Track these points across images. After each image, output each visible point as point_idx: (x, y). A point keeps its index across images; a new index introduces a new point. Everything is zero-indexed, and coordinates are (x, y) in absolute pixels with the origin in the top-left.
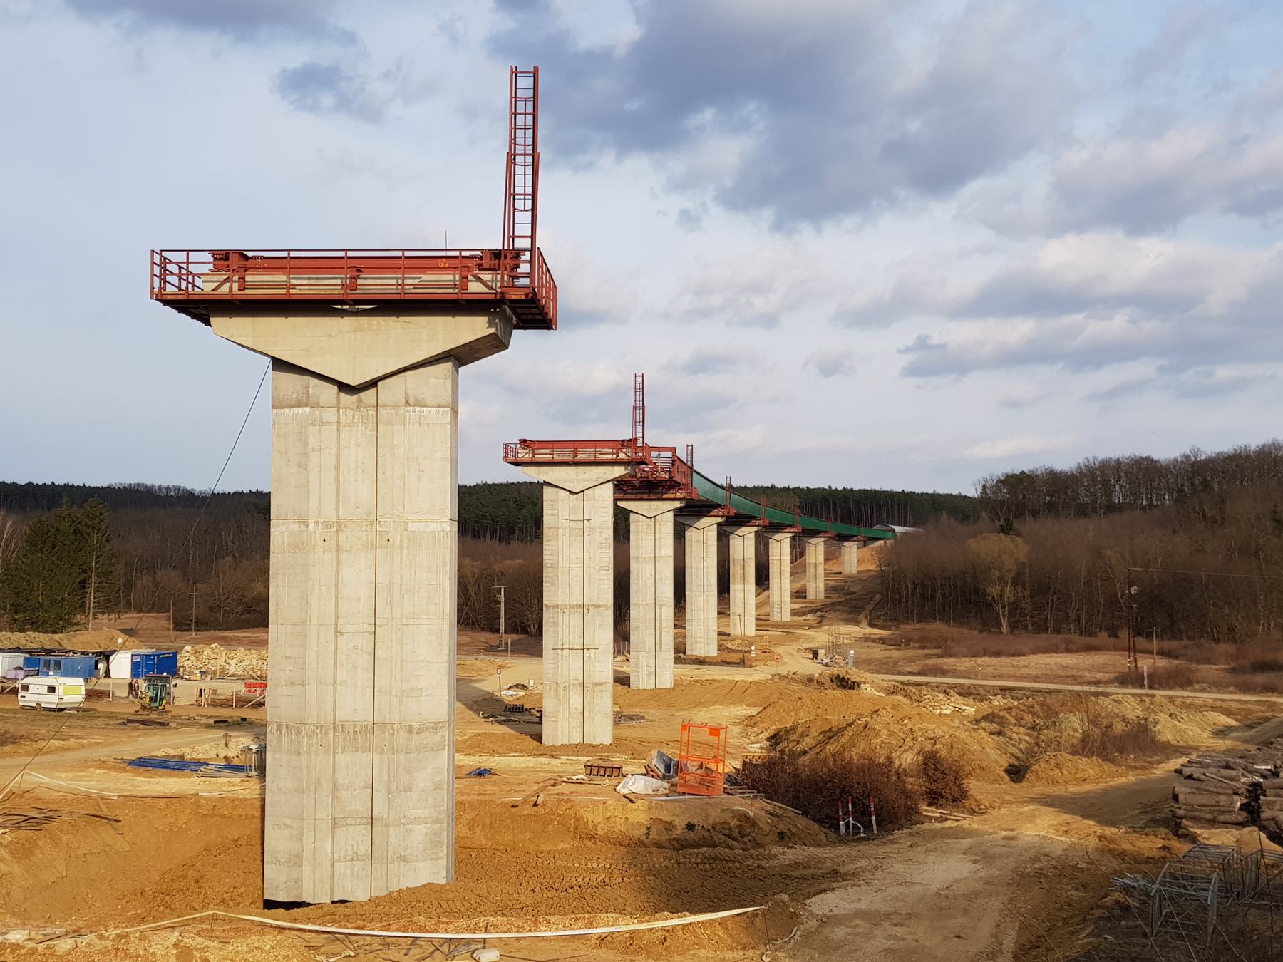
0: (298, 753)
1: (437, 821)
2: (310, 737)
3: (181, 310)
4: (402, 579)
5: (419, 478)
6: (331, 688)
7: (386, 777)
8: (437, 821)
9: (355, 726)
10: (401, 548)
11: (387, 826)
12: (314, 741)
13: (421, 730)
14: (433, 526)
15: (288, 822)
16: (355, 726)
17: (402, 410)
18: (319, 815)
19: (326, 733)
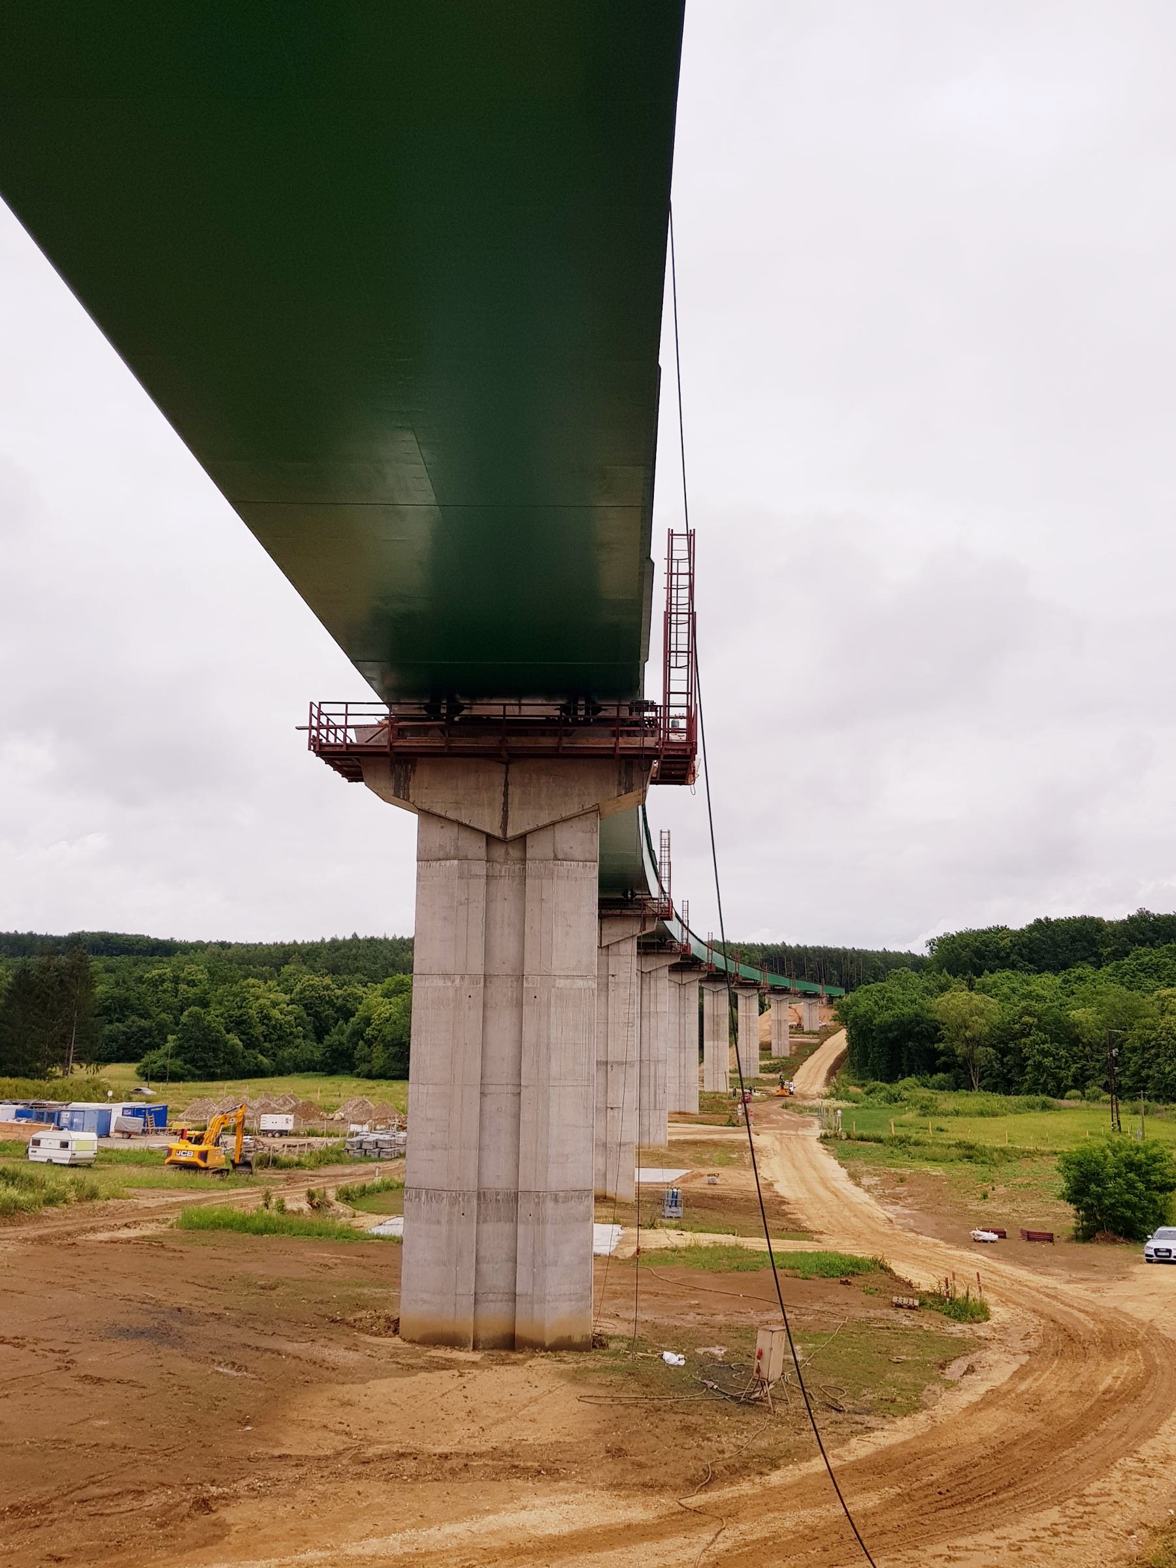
0: (439, 1222)
1: (582, 1298)
2: (452, 1204)
3: (329, 761)
4: (549, 1038)
5: (567, 933)
6: (475, 1153)
7: (530, 1250)
8: (582, 1298)
9: (498, 1194)
10: (549, 1006)
11: (532, 1303)
12: (456, 1208)
13: (566, 1200)
14: (580, 983)
15: (425, 1296)
16: (498, 1194)
17: (551, 864)
18: (460, 1290)
19: (469, 1201)
